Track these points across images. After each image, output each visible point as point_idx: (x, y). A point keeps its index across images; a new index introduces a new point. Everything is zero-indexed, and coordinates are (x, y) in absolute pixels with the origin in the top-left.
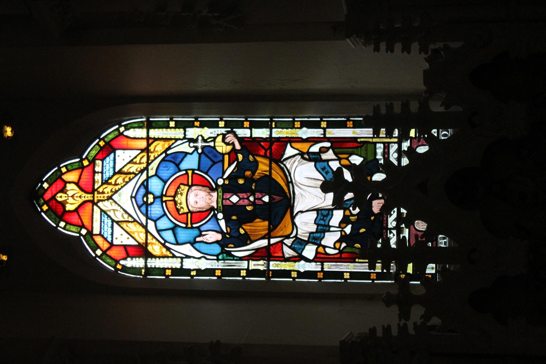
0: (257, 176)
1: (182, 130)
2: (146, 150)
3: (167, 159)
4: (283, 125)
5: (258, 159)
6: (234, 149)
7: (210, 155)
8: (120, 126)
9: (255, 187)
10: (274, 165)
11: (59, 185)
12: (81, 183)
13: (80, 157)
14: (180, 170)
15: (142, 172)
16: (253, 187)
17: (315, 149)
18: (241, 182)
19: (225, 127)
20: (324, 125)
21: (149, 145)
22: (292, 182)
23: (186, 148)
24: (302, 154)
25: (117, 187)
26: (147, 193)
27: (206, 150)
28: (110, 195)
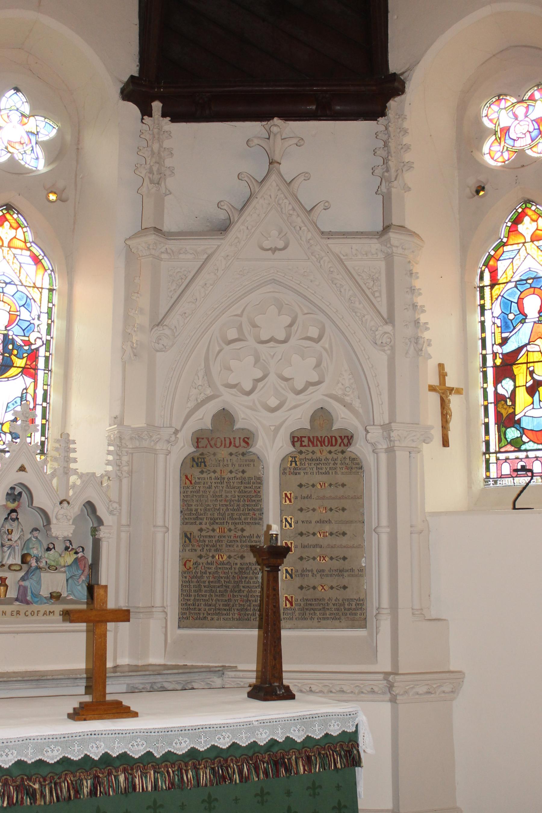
0: (13, 357)
1: (46, 311)
2: (35, 287)
3: (28, 299)
4: (46, 378)
5: (25, 359)
6: (32, 344)
7: (29, 328)
8: (51, 271)
9: (6, 356)
10: (21, 369)
11: (15, 225)
12: (15, 240)
13: (33, 242)
14: (20, 307)
15: (20, 281)
16: (6, 355)
17: (29, 398)
18: (10, 347)
19: (47, 340)
20: (45, 404)
21: (38, 288)
22: (8, 380)
23: (35, 313)
24: (26, 389)
25: (11, 263)
26: (7, 284)
27: (32, 325)
28: (6, 258)
